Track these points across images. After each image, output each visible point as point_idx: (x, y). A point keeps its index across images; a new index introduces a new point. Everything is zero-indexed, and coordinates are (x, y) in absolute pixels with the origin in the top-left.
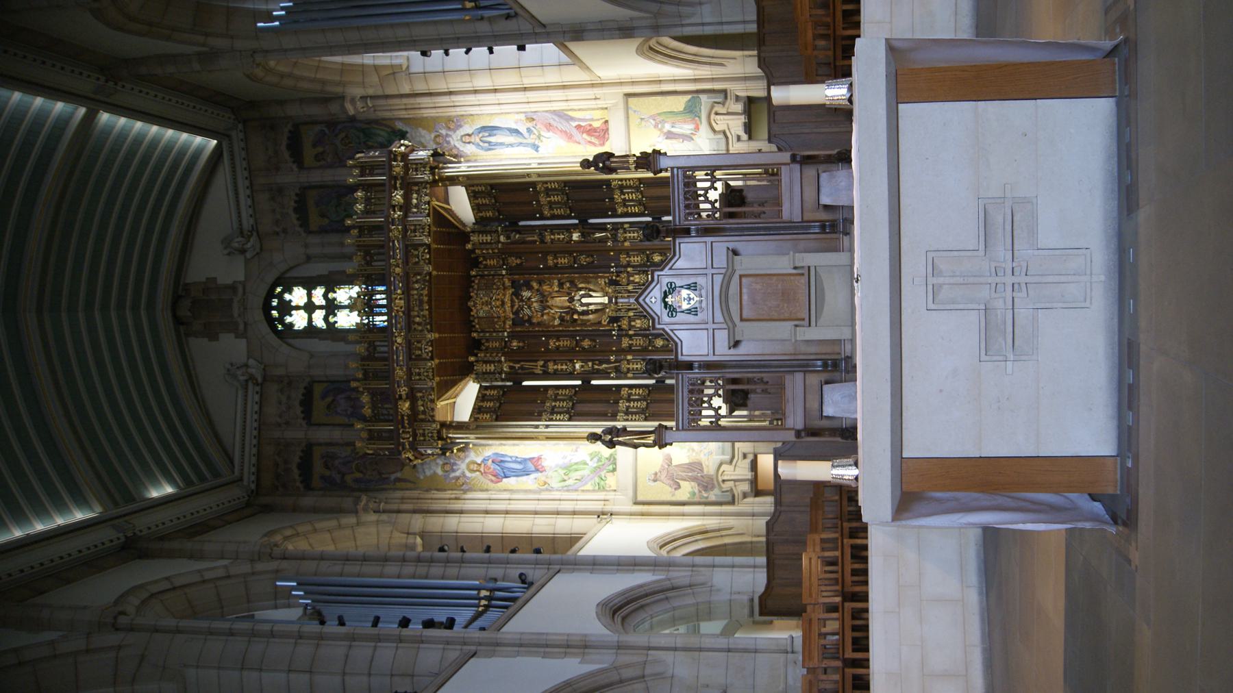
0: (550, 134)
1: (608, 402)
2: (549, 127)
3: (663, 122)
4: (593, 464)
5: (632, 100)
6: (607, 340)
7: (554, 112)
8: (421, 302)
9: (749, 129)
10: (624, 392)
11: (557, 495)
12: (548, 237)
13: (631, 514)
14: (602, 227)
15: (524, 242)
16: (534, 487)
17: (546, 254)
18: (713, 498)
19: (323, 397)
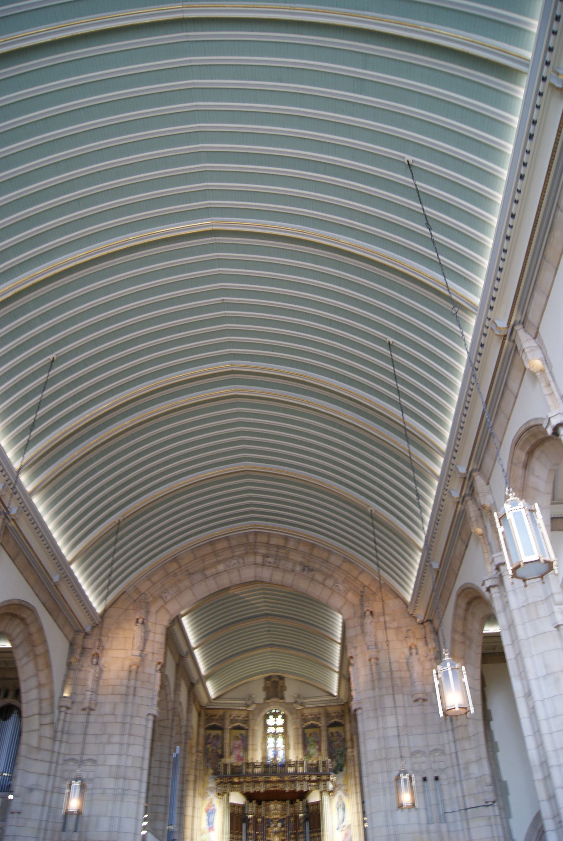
2: (346, 835)
8: (275, 787)
12: (301, 836)
17: (295, 834)
19: (241, 735)
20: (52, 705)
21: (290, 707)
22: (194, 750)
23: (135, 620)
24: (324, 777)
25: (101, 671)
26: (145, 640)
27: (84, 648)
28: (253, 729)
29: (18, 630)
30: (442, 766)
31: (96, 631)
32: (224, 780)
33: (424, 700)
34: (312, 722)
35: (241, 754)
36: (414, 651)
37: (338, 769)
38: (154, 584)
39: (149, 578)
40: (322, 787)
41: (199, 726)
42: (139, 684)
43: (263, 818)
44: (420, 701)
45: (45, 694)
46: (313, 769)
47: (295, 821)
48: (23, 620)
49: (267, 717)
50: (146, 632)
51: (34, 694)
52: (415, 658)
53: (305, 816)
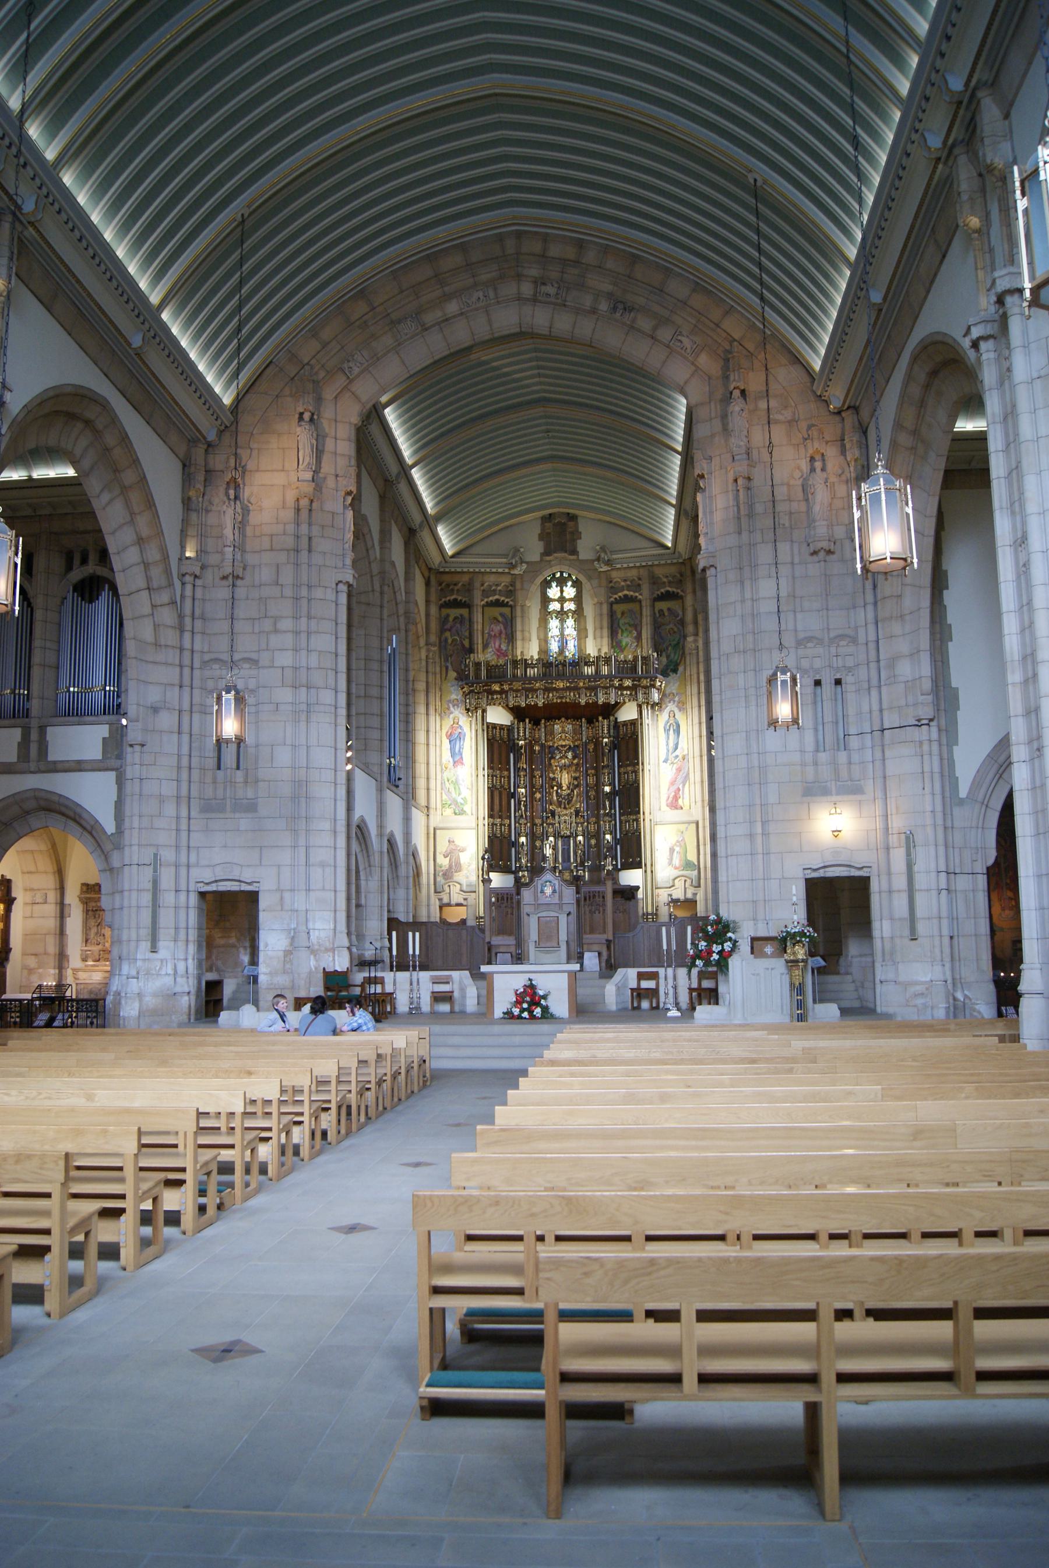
0: (674, 770)
1: (500, 811)
2: (679, 770)
3: (680, 846)
4: (460, 800)
5: (694, 826)
6: (540, 808)
7: (688, 774)
8: (562, 698)
9: (675, 902)
10: (507, 822)
11: (439, 777)
13: (428, 827)
14: (612, 806)
15: (603, 755)
16: (444, 761)
17: (596, 769)
18: (439, 879)
19: (501, 614)
20: (168, 572)
21: (587, 568)
22: (422, 642)
23: (297, 416)
24: (645, 682)
25: (246, 511)
26: (319, 453)
28: (522, 606)
29: (83, 442)
30: (850, 662)
31: (227, 438)
32: (477, 688)
33: (829, 552)
34: (626, 592)
35: (504, 647)
36: (818, 465)
37: (670, 669)
38: (325, 345)
39: (314, 333)
40: (640, 696)
41: (428, 602)
42: (315, 531)
43: (542, 746)
44: (822, 554)
45: (153, 554)
46: (628, 669)
47: (595, 750)
48: (88, 423)
49: (547, 584)
51: (132, 555)
52: (819, 477)
53: (612, 742)
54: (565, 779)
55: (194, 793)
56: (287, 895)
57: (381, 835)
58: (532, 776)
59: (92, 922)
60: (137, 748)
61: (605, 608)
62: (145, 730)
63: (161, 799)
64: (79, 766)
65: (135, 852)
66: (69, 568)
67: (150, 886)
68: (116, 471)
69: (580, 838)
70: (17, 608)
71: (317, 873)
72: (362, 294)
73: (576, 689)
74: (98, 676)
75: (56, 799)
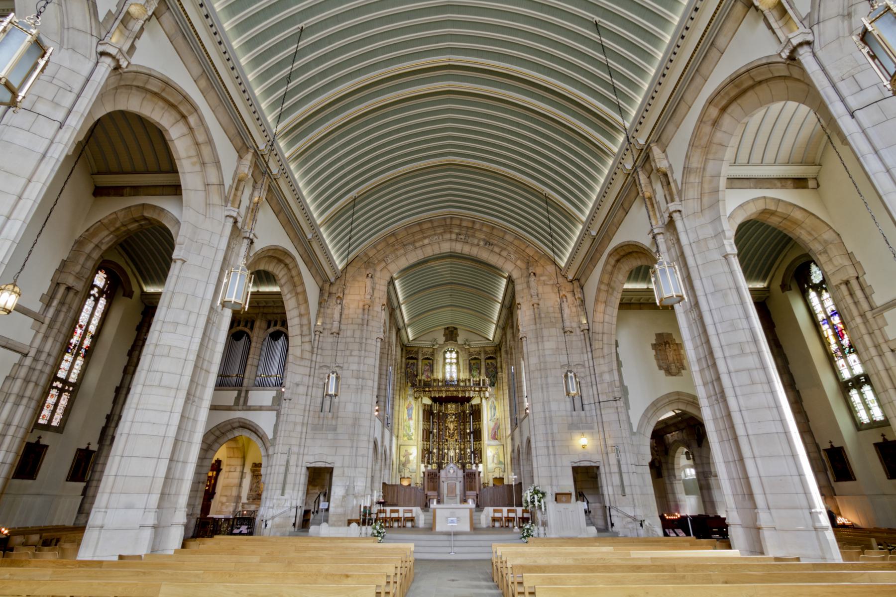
2: (496, 424)
14: (470, 438)
20: (310, 329)
21: (461, 347)
24: (484, 389)
26: (373, 289)
27: (330, 293)
29: (283, 273)
31: (338, 281)
33: (571, 332)
36: (565, 300)
38: (378, 251)
41: (402, 357)
42: (370, 317)
45: (305, 321)
48: (286, 265)
49: (445, 352)
50: (374, 283)
54: (452, 426)
55: (310, 422)
56: (346, 469)
57: (382, 446)
58: (439, 425)
59: (255, 481)
60: (288, 401)
61: (468, 361)
62: (292, 393)
63: (295, 423)
64: (261, 408)
65: (280, 448)
66: (269, 327)
67: (285, 463)
68: (295, 286)
69: (457, 451)
70: (247, 307)
71: (360, 459)
72: (393, 234)
73: (458, 391)
74: (274, 370)
75: (248, 422)
